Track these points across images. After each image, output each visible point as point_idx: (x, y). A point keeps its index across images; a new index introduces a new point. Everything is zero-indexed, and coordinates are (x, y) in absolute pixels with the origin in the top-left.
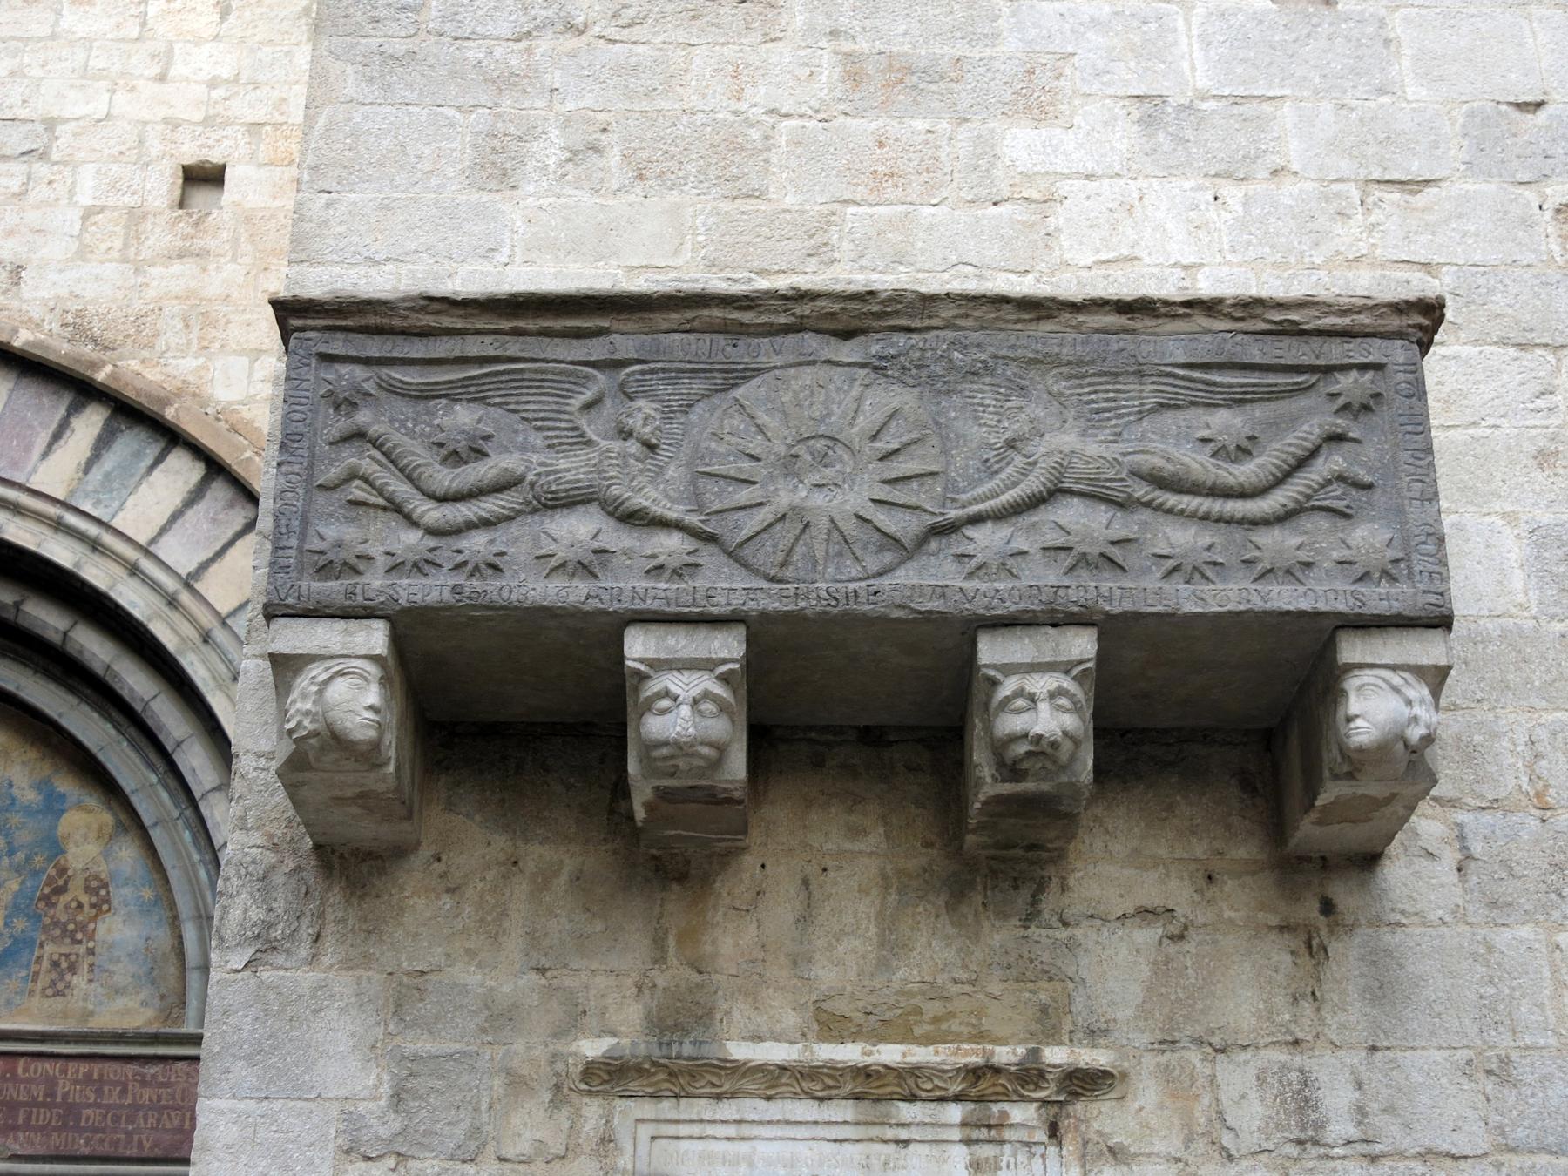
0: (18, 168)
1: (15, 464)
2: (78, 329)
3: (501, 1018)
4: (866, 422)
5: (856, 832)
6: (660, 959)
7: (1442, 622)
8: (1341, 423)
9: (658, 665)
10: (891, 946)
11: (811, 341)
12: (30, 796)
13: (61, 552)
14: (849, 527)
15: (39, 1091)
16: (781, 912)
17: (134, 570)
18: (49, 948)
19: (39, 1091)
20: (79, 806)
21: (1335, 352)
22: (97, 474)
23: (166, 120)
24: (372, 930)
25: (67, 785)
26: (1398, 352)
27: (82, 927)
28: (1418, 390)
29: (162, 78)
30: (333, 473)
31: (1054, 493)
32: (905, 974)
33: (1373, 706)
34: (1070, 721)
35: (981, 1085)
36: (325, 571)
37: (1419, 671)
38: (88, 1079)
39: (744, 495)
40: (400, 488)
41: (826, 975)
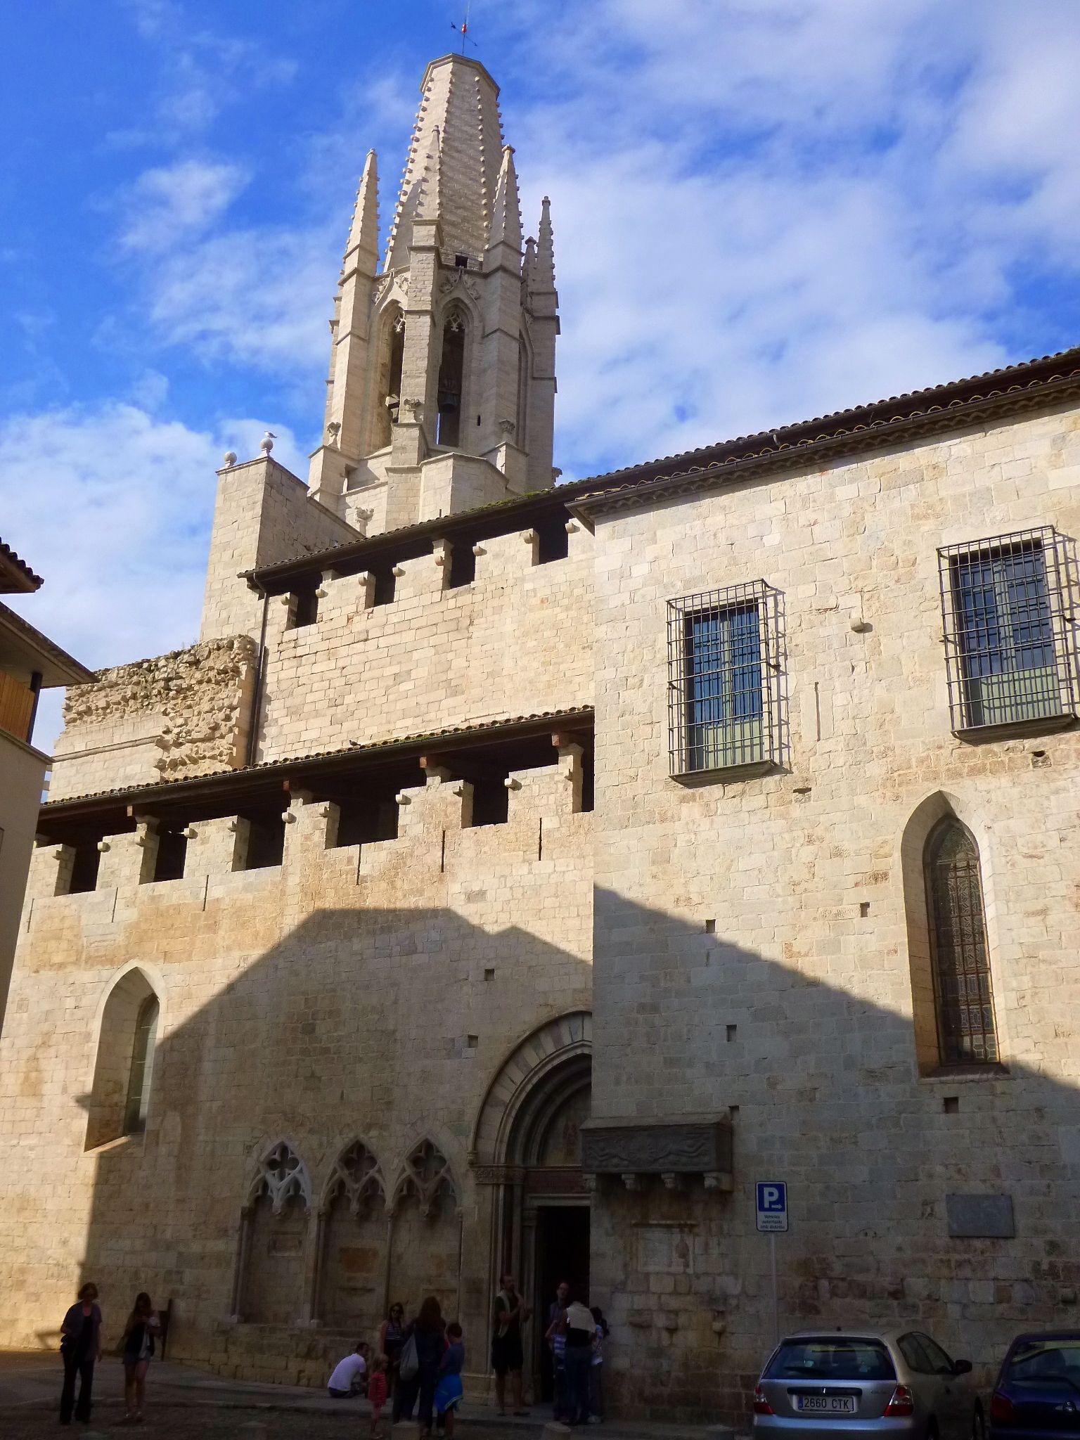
31: (670, 1153)
35: (680, 1226)
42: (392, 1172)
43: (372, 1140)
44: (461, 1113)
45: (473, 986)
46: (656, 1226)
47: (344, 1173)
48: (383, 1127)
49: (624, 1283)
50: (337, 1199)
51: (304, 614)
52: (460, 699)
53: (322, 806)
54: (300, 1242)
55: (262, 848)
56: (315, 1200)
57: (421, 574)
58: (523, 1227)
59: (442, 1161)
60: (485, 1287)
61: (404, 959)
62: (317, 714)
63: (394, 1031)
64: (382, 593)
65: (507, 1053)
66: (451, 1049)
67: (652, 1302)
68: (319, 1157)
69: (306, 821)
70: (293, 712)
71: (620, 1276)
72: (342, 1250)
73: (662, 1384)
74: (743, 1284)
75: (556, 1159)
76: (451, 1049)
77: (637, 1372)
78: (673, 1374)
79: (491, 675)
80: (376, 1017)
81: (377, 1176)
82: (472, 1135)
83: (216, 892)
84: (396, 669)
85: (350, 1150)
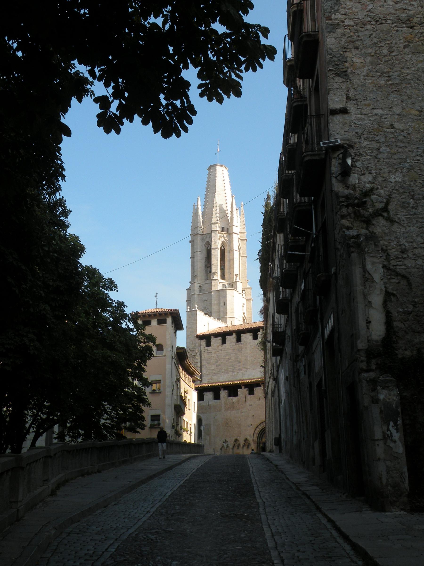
42: (242, 442)
47: (235, 443)
51: (209, 344)
52: (240, 364)
53: (226, 391)
55: (217, 397)
56: (231, 446)
57: (231, 339)
62: (214, 364)
64: (224, 342)
66: (249, 426)
69: (224, 394)
70: (209, 363)
76: (249, 426)
79: (246, 360)
83: (210, 403)
84: (228, 357)
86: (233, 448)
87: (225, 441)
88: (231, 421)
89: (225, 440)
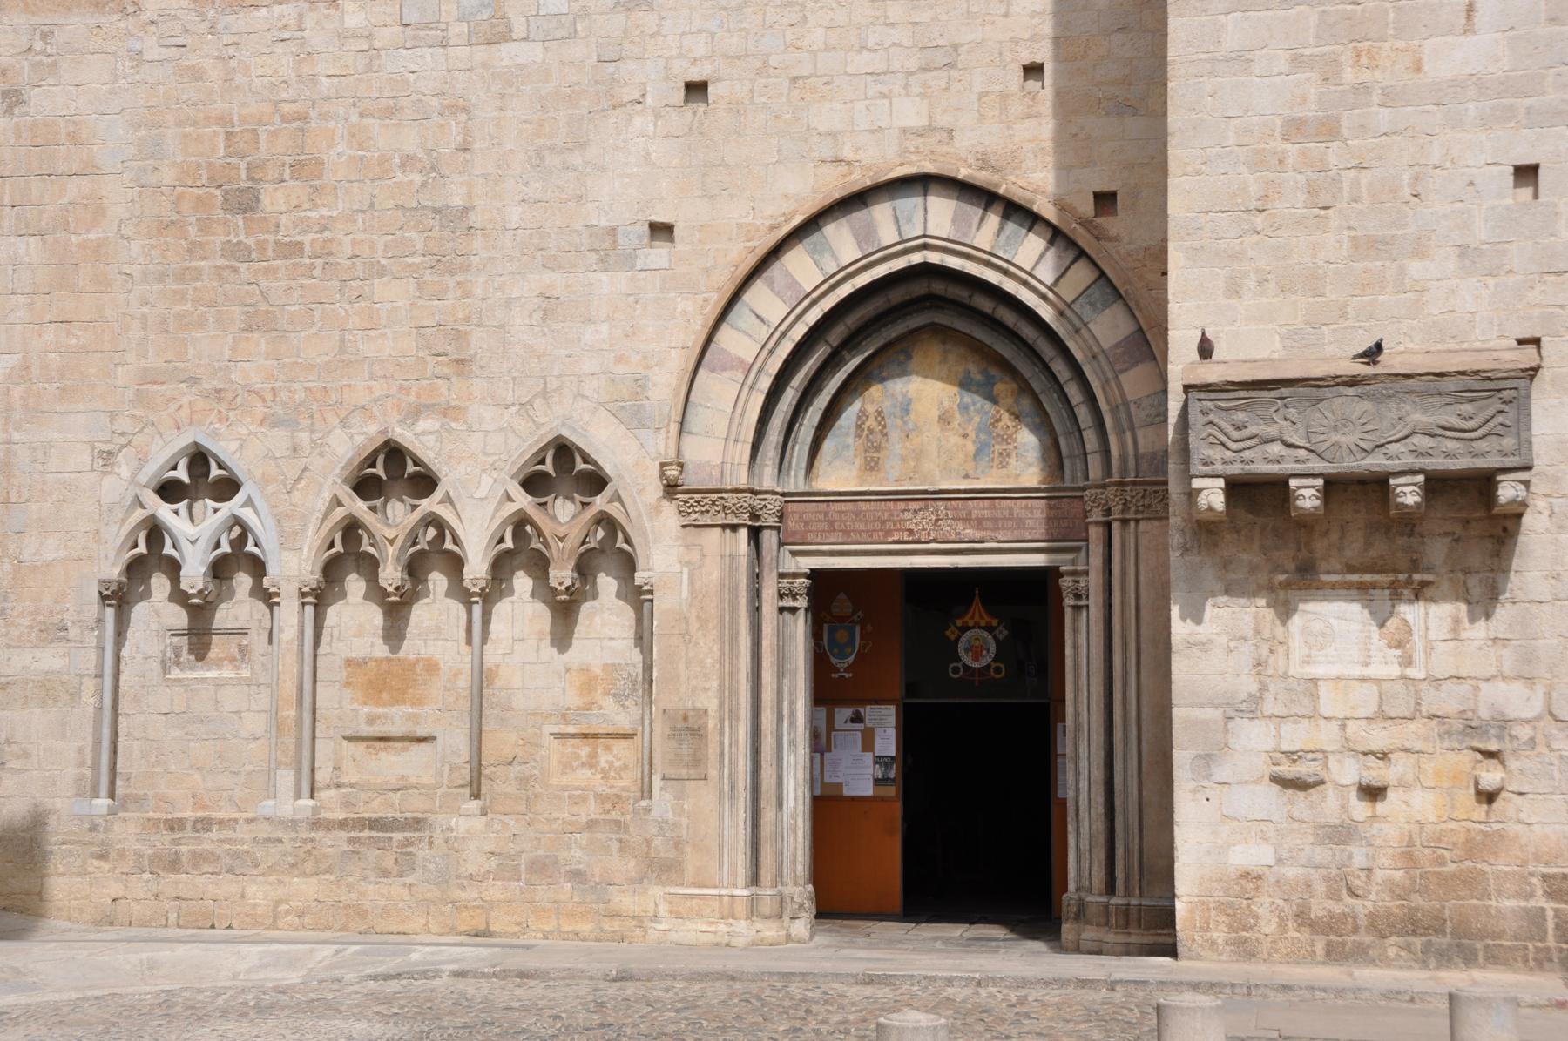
0: (943, 74)
1: (965, 235)
2: (984, 163)
3: (1253, 569)
4: (1356, 414)
5: (1357, 512)
6: (1299, 550)
7: (1528, 468)
8: (1502, 407)
9: (1299, 488)
10: (1368, 545)
11: (1341, 388)
12: (979, 377)
13: (992, 277)
14: (1354, 448)
15: (1006, 513)
16: (1334, 536)
17: (1025, 283)
18: (997, 447)
19: (1006, 513)
20: (1001, 380)
21: (1502, 384)
22: (1003, 237)
23: (1011, 40)
24: (1216, 545)
25: (993, 371)
26: (1522, 384)
27: (1010, 436)
28: (1528, 396)
29: (1006, 15)
30: (1204, 435)
32: (1373, 553)
33: (1507, 491)
34: (1417, 499)
36: (1206, 464)
37: (1521, 482)
38: (1026, 507)
39: (1322, 438)
40: (1224, 439)
41: (1348, 553)
43: (422, 439)
44: (640, 383)
45: (657, 116)
46: (1333, 586)
47: (359, 507)
48: (447, 412)
49: (1256, 700)
50: (348, 554)
54: (243, 650)
56: (293, 564)
58: (781, 610)
59: (596, 482)
60: (712, 723)
61: (481, 53)
63: (466, 210)
65: (751, 261)
66: (608, 249)
67: (1326, 736)
68: (293, 474)
71: (1249, 685)
72: (349, 662)
73: (1353, 893)
74: (1548, 696)
75: (839, 473)
77: (1291, 872)
78: (1379, 875)
80: (418, 179)
81: (445, 513)
82: (674, 428)
85: (371, 461)
86: (322, 595)
87: (200, 477)
88: (304, 168)
89: (199, 459)
